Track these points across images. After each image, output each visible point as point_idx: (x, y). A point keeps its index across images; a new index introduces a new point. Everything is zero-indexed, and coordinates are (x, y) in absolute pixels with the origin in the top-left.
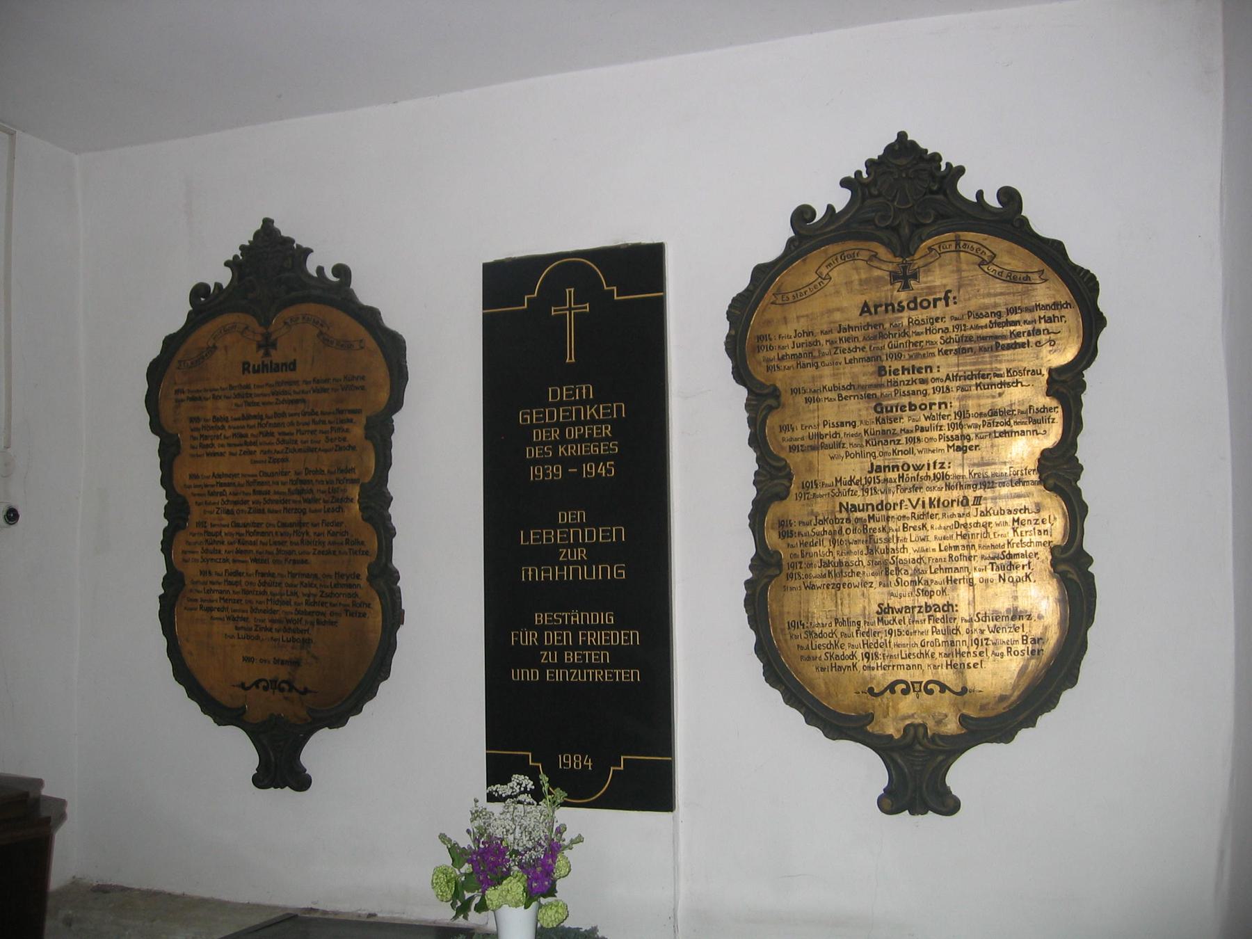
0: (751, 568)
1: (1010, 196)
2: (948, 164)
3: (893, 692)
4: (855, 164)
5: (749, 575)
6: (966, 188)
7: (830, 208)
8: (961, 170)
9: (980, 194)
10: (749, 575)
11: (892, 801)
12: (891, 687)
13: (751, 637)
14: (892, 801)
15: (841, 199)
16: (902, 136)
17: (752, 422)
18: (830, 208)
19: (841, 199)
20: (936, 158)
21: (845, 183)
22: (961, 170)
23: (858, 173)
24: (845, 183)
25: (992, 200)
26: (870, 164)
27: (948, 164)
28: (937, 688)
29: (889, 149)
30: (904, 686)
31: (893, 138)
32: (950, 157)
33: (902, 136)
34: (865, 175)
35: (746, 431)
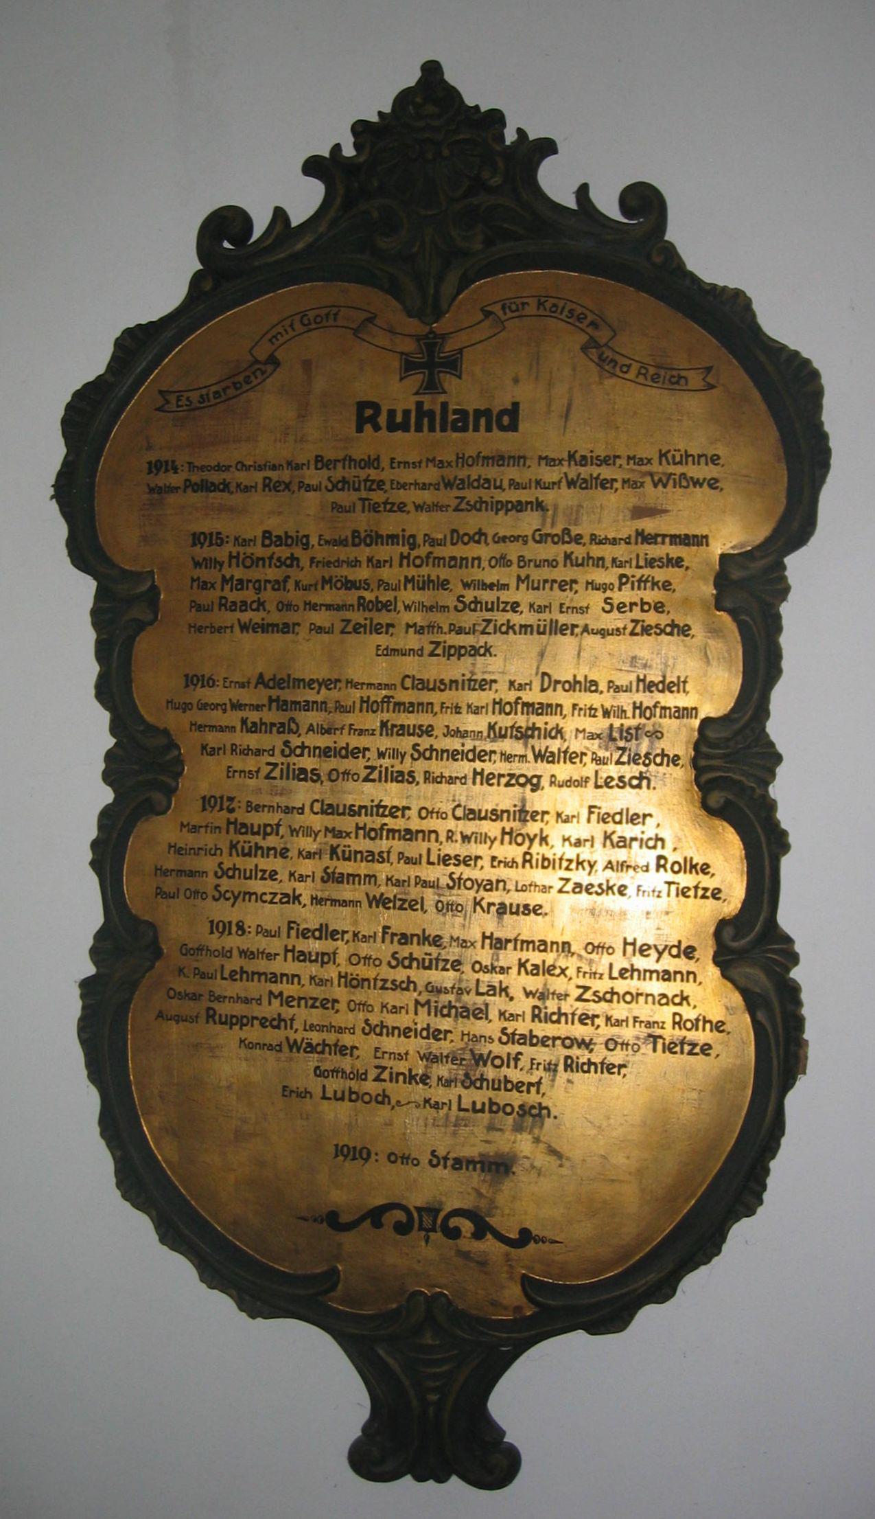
0: (95, 953)
1: (645, 201)
2: (521, 132)
3: (377, 1224)
4: (334, 135)
5: (90, 970)
6: (557, 181)
7: (280, 215)
8: (547, 147)
9: (583, 192)
10: (90, 970)
11: (375, 1457)
12: (376, 1216)
13: (90, 1100)
14: (375, 1457)
15: (305, 200)
16: (432, 70)
17: (103, 651)
18: (280, 215)
19: (305, 200)
20: (496, 118)
21: (313, 167)
22: (547, 147)
23: (337, 148)
24: (313, 167)
25: (608, 204)
26: (361, 129)
27: (521, 132)
28: (467, 1226)
29: (403, 99)
30: (400, 1215)
31: (411, 77)
32: (524, 120)
33: (432, 70)
34: (349, 151)
35: (91, 669)
